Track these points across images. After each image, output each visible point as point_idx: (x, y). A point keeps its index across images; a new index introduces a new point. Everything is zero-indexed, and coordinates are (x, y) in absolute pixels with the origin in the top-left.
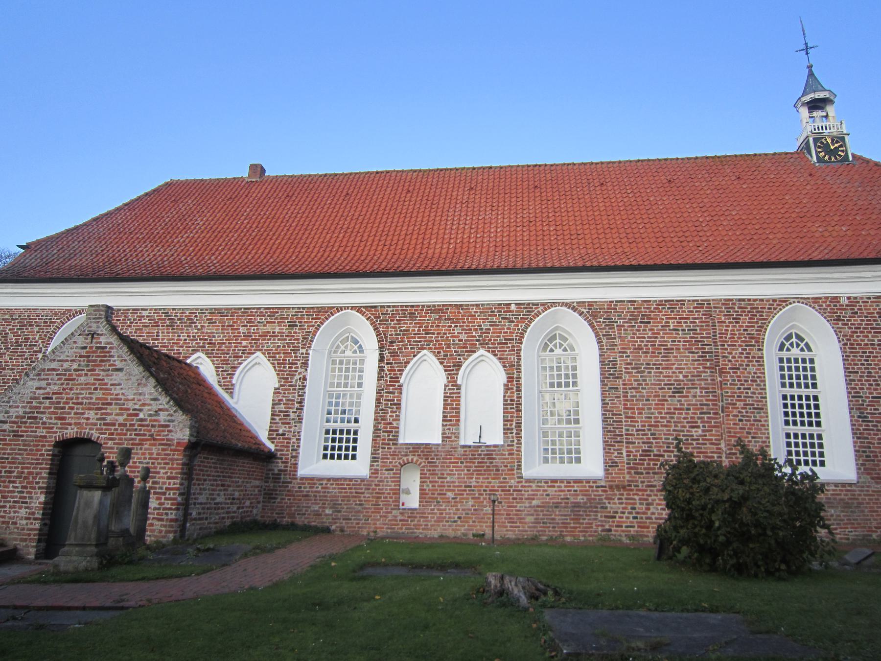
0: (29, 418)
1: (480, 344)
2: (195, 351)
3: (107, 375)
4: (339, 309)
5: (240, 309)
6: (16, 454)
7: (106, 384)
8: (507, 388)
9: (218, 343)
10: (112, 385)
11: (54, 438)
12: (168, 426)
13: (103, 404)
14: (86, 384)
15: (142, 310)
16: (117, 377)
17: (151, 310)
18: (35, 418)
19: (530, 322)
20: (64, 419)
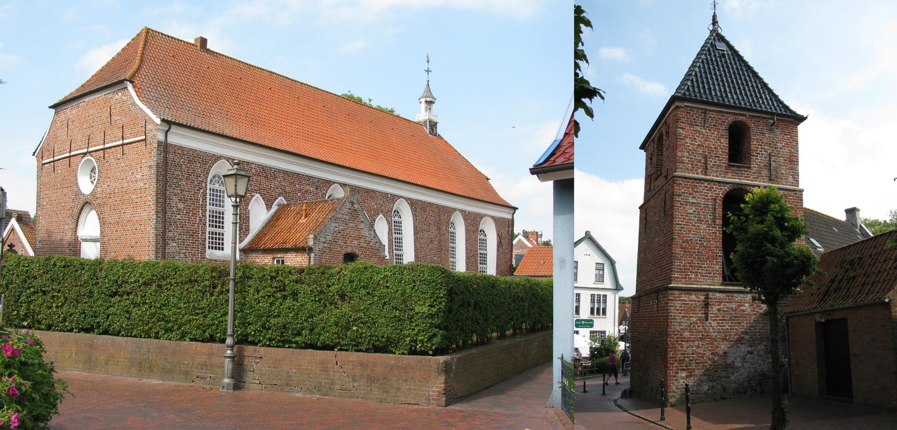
0: (334, 241)
1: (381, 211)
2: (279, 195)
3: (359, 224)
4: (334, 183)
5: (295, 173)
6: (331, 259)
7: (359, 228)
8: (389, 234)
9: (289, 192)
10: (361, 229)
11: (343, 252)
12: (379, 250)
13: (359, 238)
14: (352, 227)
15: (251, 163)
16: (362, 225)
17: (255, 164)
18: (336, 242)
19: (394, 203)
20: (346, 243)
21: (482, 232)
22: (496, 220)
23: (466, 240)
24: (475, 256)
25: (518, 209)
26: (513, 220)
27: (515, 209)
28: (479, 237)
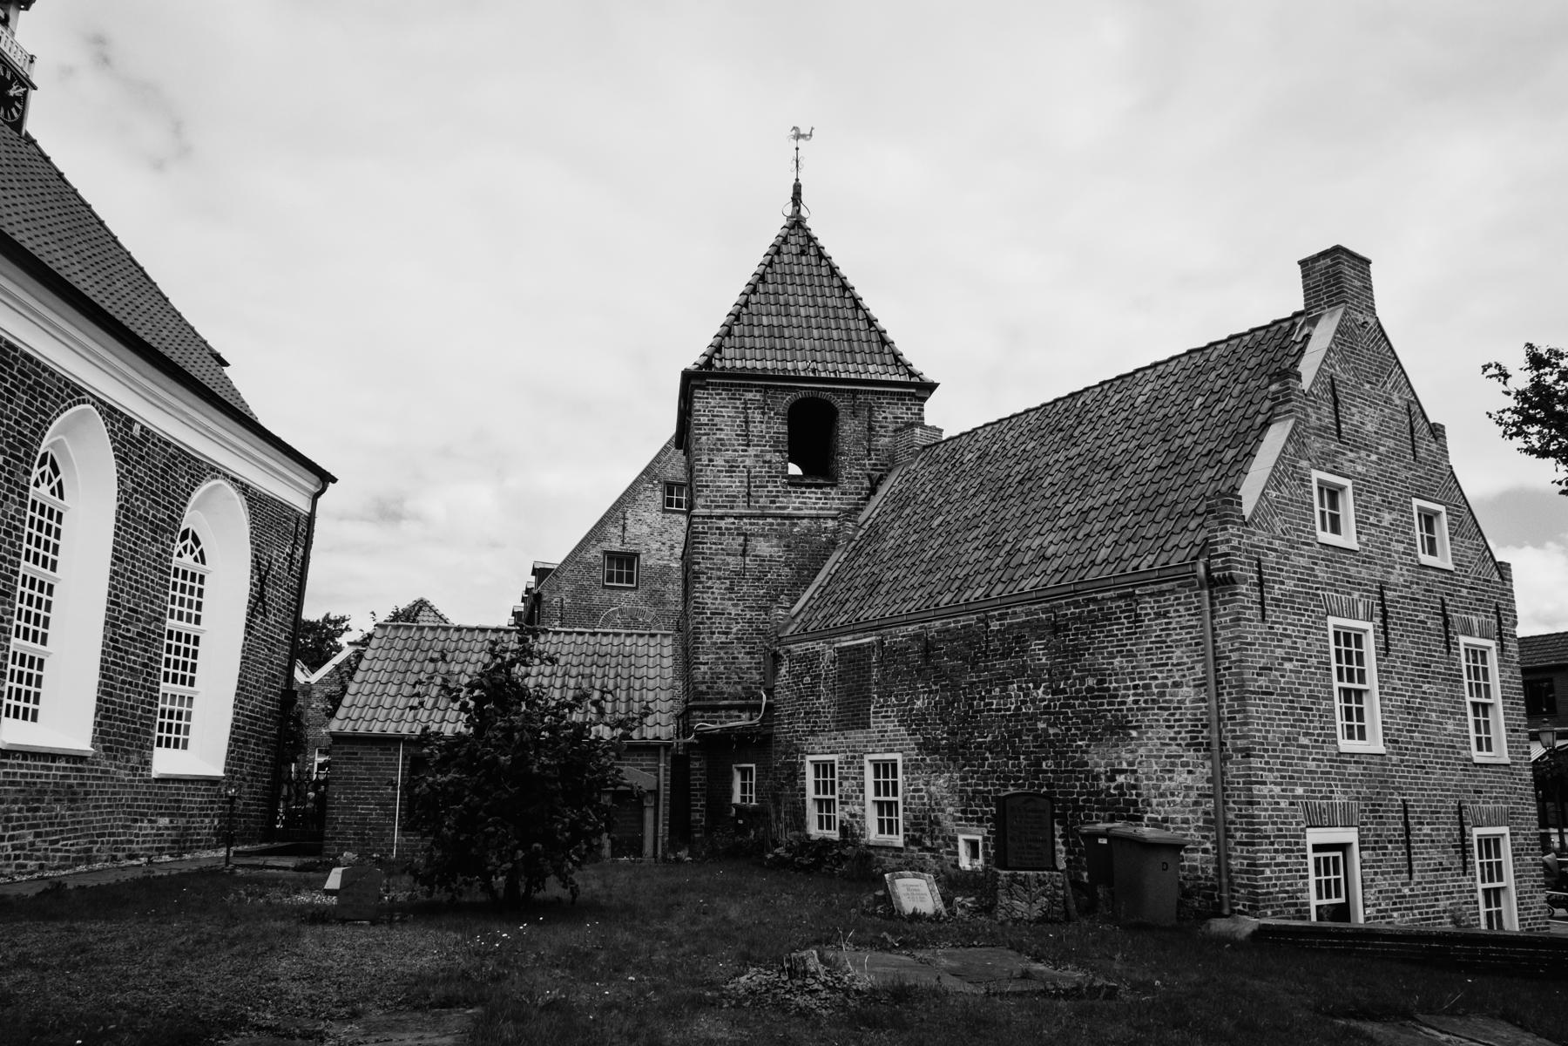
21: (189, 541)
22: (256, 501)
23: (117, 558)
24: (148, 638)
25: (334, 480)
26: (311, 519)
27: (325, 478)
28: (176, 562)
